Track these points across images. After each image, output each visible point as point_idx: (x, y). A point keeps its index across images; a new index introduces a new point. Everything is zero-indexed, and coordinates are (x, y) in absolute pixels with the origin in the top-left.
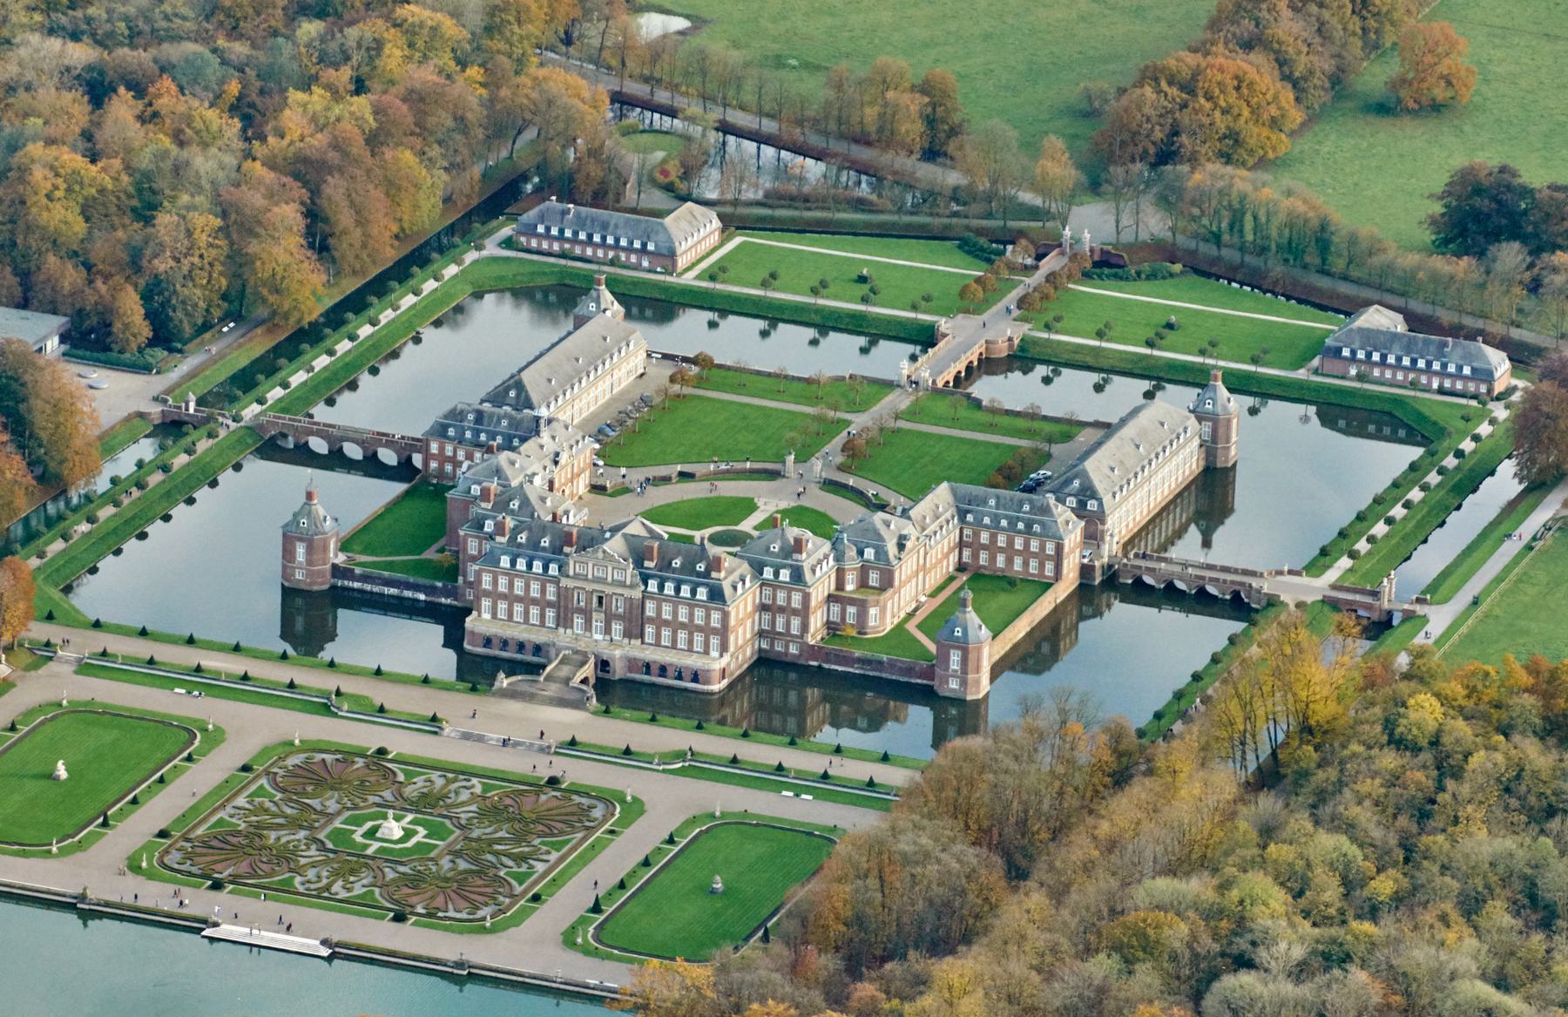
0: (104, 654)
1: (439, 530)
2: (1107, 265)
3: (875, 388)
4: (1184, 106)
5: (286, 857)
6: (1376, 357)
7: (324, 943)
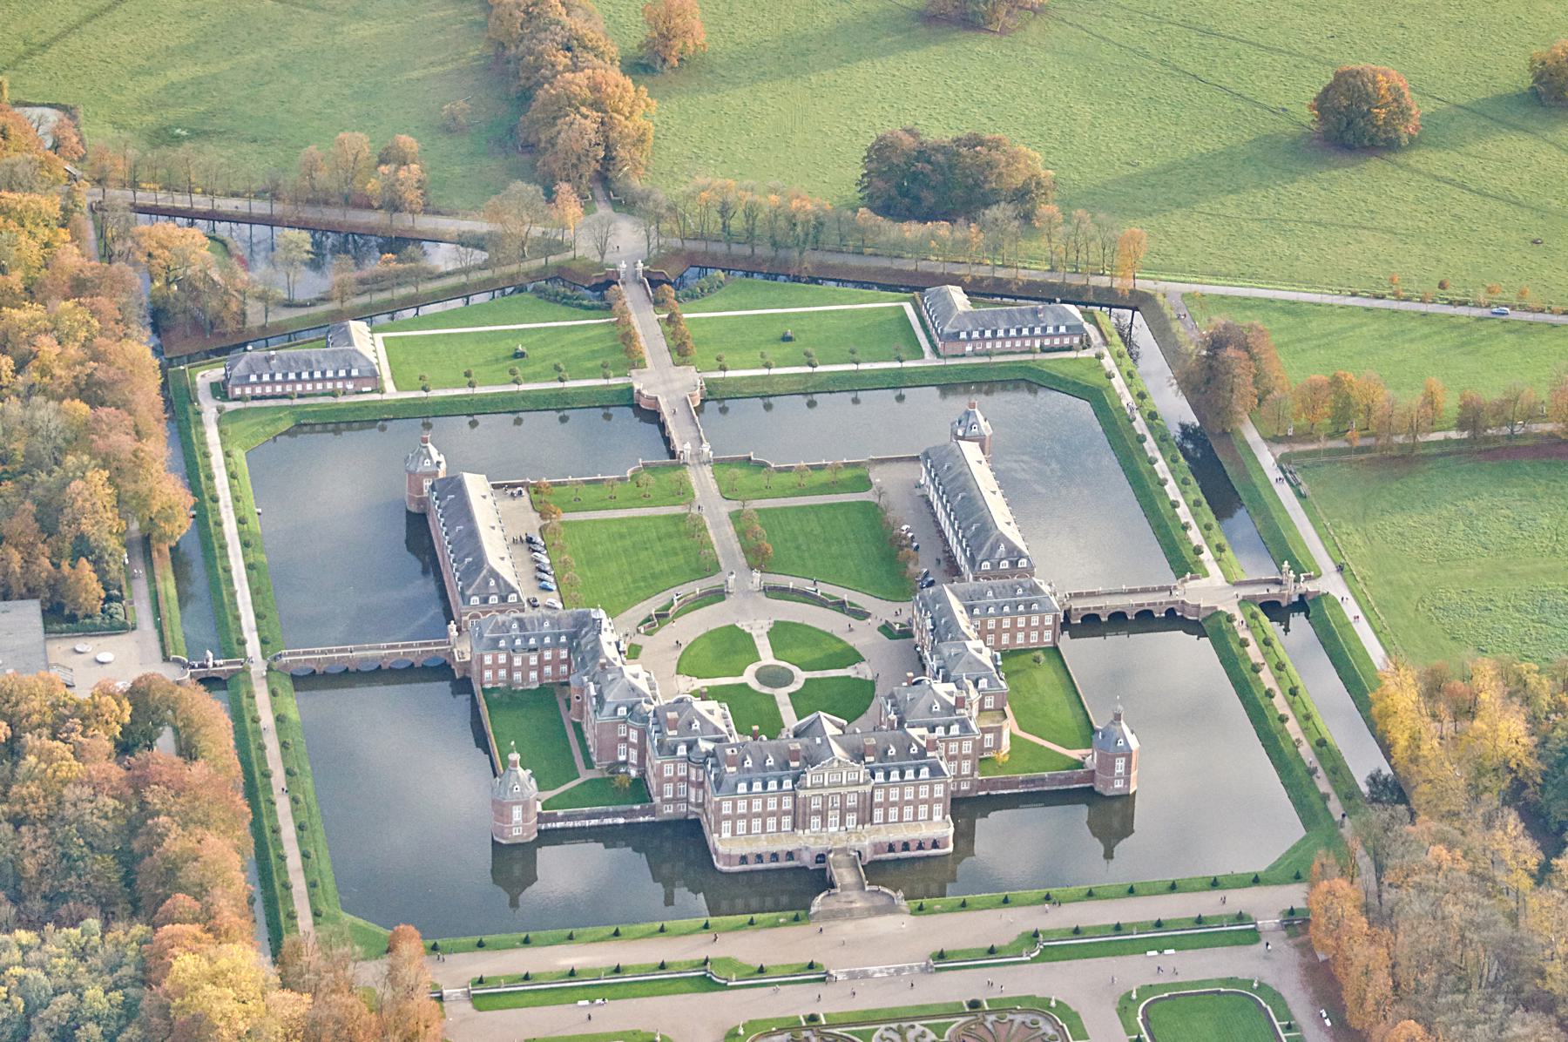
0: (481, 981)
6: (988, 334)
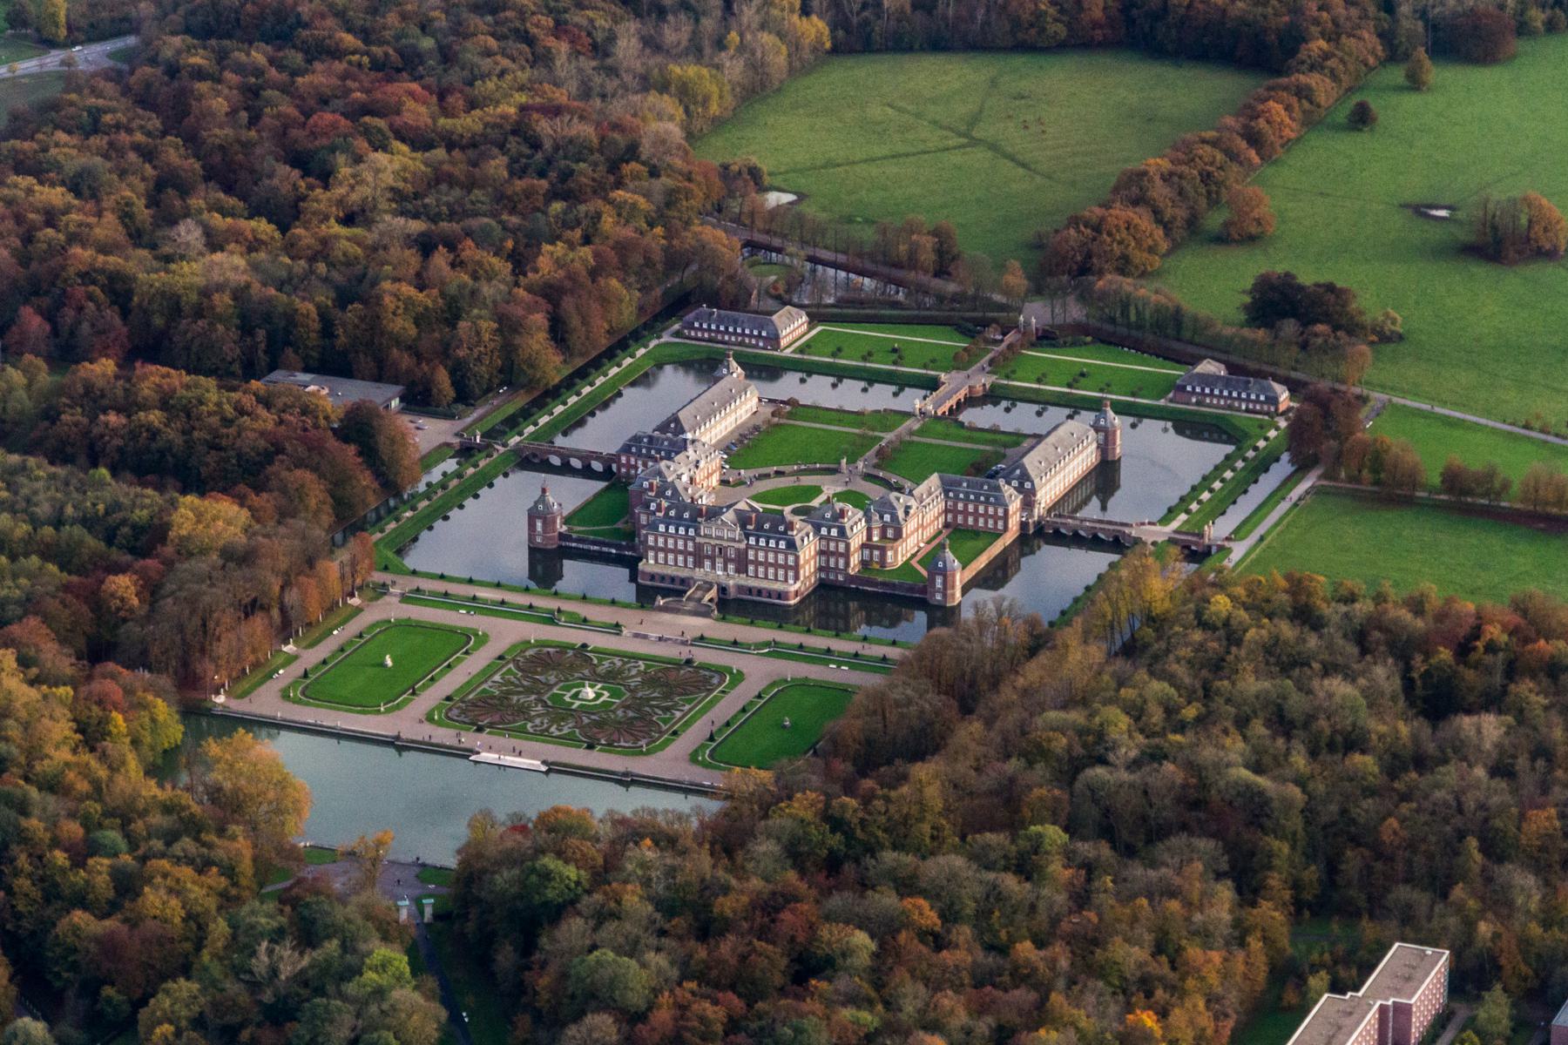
1: (625, 510)
2: (1046, 338)
3: (897, 417)
4: (1094, 239)
5: (523, 711)
6: (1207, 391)
7: (544, 762)
